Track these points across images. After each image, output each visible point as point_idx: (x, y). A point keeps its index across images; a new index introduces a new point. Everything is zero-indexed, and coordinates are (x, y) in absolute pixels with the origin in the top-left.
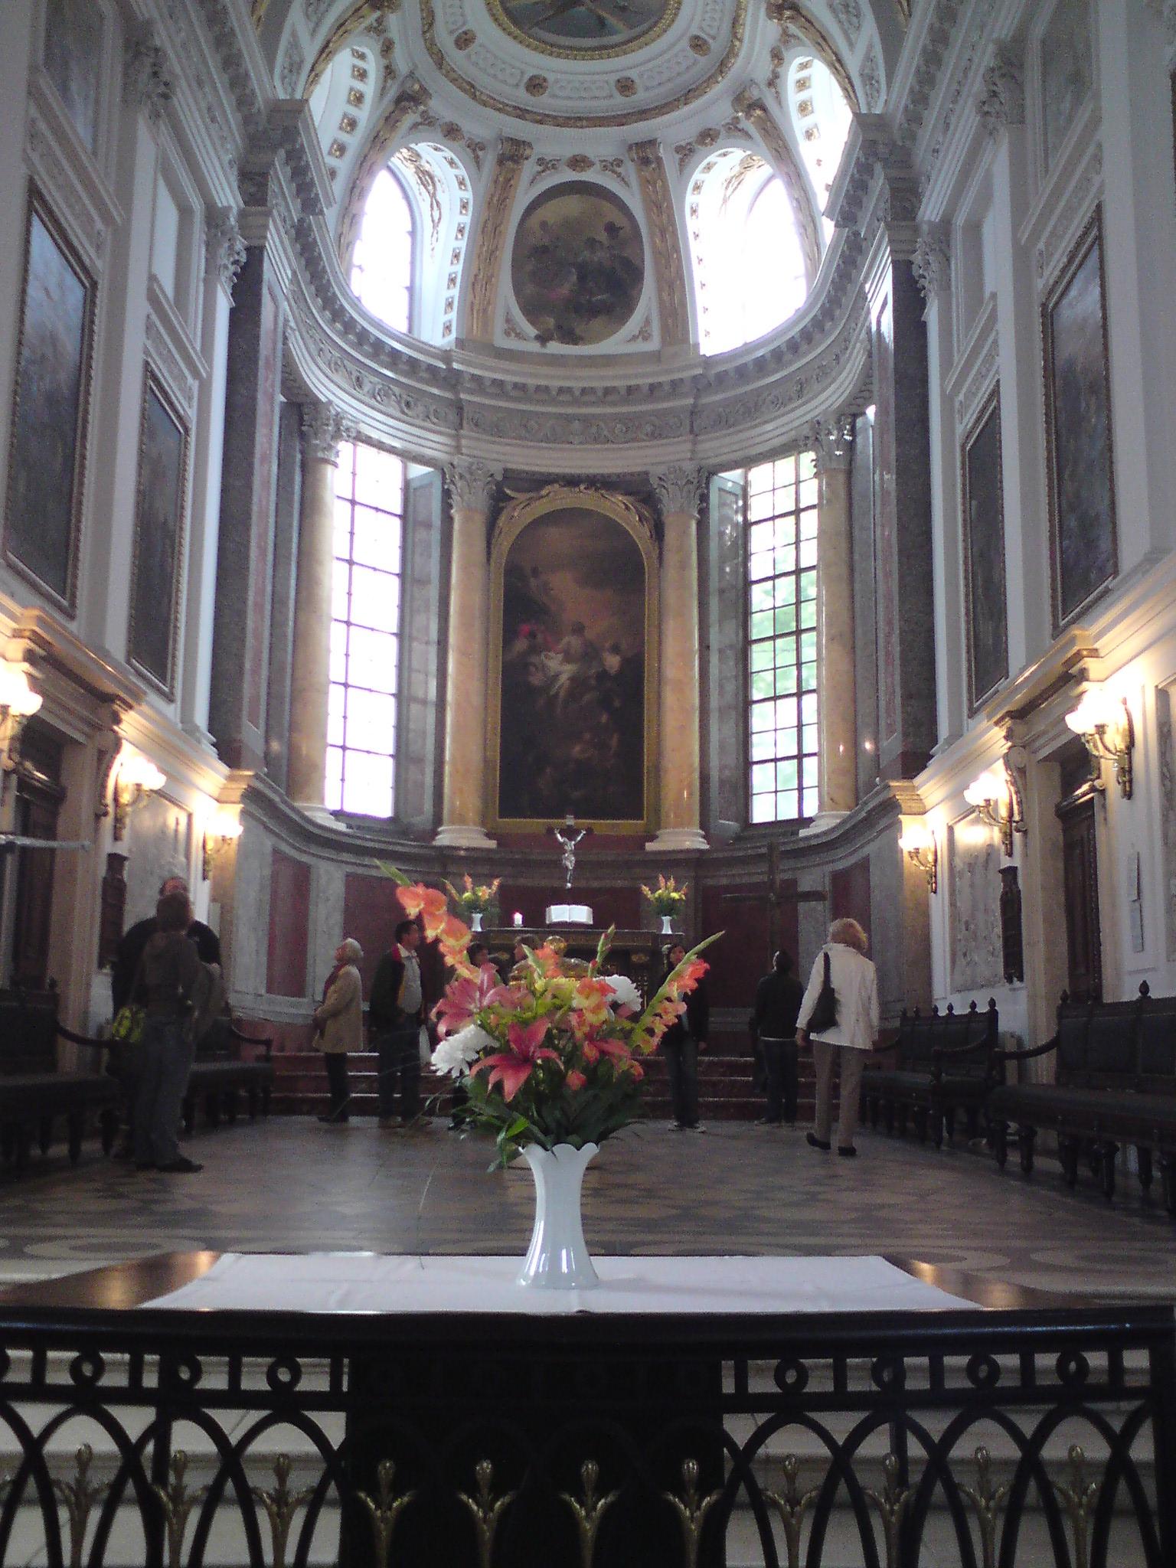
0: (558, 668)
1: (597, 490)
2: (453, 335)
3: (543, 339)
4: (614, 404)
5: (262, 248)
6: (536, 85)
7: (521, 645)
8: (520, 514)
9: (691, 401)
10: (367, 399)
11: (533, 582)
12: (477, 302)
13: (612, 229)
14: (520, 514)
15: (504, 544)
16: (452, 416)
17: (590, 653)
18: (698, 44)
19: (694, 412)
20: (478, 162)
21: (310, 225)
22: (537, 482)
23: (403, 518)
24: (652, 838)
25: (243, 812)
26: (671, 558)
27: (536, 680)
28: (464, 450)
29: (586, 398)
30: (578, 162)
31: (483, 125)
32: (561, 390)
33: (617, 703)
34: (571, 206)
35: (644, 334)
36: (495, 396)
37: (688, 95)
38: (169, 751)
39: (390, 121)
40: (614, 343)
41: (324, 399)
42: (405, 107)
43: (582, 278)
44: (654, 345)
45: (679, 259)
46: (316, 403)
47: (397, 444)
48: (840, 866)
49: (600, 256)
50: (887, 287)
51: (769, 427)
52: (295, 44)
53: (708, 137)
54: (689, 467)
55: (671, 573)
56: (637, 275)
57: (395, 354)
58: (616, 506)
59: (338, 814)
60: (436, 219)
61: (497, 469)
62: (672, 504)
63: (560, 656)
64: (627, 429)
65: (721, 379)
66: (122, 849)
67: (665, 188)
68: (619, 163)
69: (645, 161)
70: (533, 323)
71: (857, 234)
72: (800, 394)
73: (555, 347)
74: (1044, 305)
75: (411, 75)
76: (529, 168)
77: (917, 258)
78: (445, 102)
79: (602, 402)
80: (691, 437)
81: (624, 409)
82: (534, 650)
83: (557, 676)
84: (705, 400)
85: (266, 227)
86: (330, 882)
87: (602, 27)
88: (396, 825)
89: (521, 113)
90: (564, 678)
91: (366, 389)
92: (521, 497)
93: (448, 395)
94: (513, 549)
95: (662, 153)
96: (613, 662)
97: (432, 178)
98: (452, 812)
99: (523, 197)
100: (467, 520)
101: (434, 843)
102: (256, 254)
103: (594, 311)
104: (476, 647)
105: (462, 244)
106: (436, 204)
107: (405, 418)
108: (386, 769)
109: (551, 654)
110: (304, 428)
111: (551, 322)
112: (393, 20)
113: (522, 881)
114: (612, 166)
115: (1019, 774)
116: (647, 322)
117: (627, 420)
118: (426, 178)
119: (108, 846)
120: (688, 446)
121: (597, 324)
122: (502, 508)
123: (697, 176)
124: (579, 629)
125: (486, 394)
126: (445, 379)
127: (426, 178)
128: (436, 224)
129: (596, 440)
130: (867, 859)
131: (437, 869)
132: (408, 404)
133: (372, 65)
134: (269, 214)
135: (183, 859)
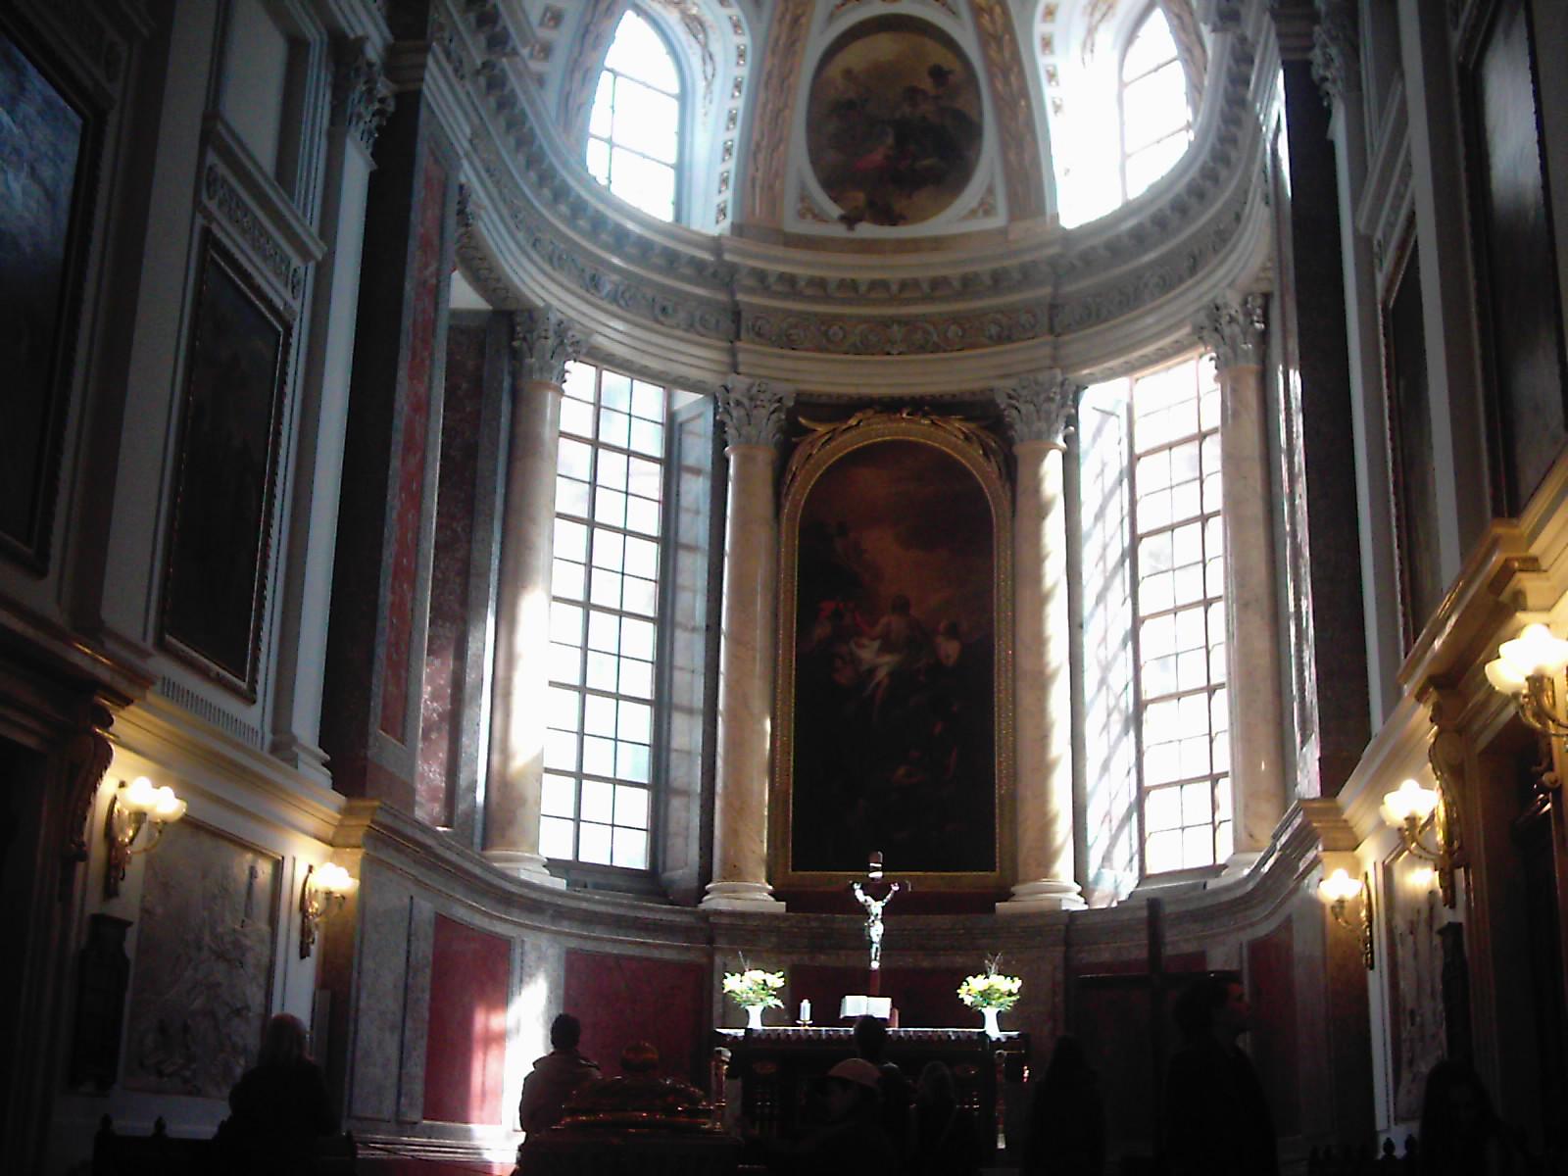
1: (925, 415)
3: (850, 220)
5: (417, 95)
7: (822, 630)
9: (1046, 291)
10: (605, 304)
12: (759, 175)
13: (939, 74)
15: (800, 492)
16: (727, 324)
19: (1054, 308)
21: (503, 70)
24: (1007, 896)
28: (741, 369)
29: (906, 295)
32: (874, 285)
34: (884, 47)
36: (785, 296)
40: (951, 220)
41: (541, 304)
44: (998, 220)
45: (1029, 106)
47: (655, 364)
48: (1262, 930)
50: (1278, 107)
51: (1150, 320)
56: (972, 131)
59: (554, 866)
60: (710, 77)
61: (786, 389)
63: (876, 644)
64: (964, 330)
67: (1006, 12)
70: (835, 200)
71: (1243, 40)
72: (1193, 270)
73: (866, 230)
74: (1462, 68)
77: (1317, 55)
79: (926, 299)
80: (1050, 338)
83: (872, 671)
84: (1070, 288)
85: (423, 66)
88: (650, 882)
91: (604, 292)
92: (821, 429)
93: (722, 297)
96: (950, 649)
97: (701, 24)
98: (724, 862)
100: (744, 461)
101: (702, 906)
104: (760, 636)
106: (708, 57)
107: (657, 326)
108: (636, 806)
109: (865, 641)
110: (516, 344)
111: (860, 198)
113: (822, 959)
115: (1453, 773)
116: (990, 190)
122: (796, 445)
124: (902, 606)
125: (775, 295)
126: (715, 275)
129: (922, 349)
130: (1289, 919)
132: (664, 310)
134: (427, 49)
135: (264, 927)
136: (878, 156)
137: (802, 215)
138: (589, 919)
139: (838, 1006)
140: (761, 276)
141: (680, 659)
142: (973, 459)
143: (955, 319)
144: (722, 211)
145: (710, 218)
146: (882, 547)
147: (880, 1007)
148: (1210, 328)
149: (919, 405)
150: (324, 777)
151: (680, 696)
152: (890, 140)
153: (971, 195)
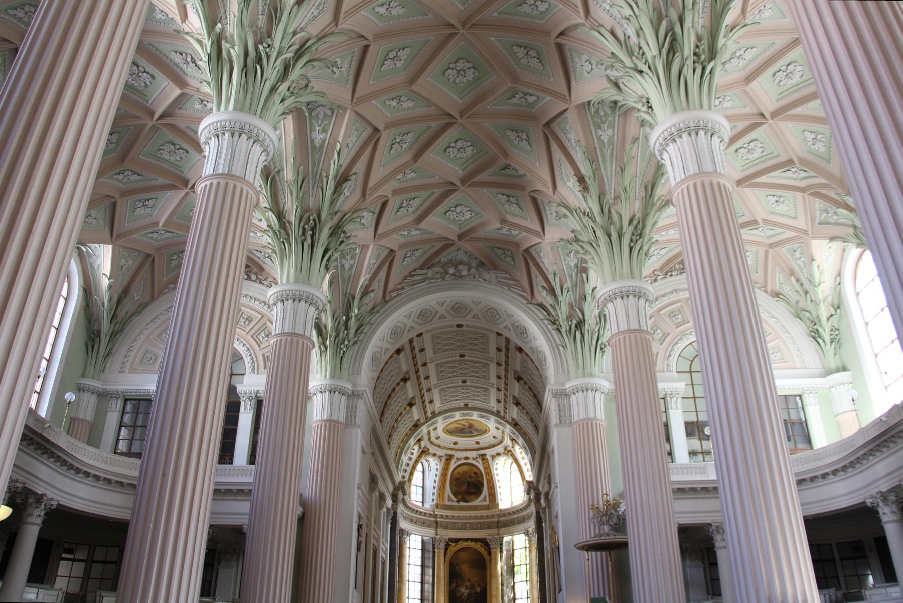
0: (464, 591)
3: (458, 502)
6: (455, 443)
7: (454, 585)
9: (496, 520)
13: (475, 473)
14: (454, 548)
18: (494, 437)
19: (498, 522)
22: (456, 541)
23: (422, 550)
26: (493, 562)
27: (458, 595)
30: (466, 458)
35: (484, 500)
37: (493, 446)
39: (420, 457)
42: (424, 452)
43: (468, 485)
44: (487, 503)
53: (498, 454)
56: (482, 485)
57: (421, 512)
58: (478, 546)
65: (504, 515)
73: (461, 504)
76: (453, 460)
82: (457, 586)
89: (452, 449)
96: (478, 589)
99: (452, 466)
102: (395, 513)
103: (471, 494)
105: (437, 479)
106: (429, 466)
111: (460, 497)
114: (474, 459)
118: (428, 461)
121: (472, 497)
124: (469, 581)
127: (428, 461)
128: (430, 471)
133: (416, 447)
141: (426, 590)
143: (479, 523)
146: (465, 569)
148: (527, 533)
149: (472, 540)
151: (426, 598)
153: (482, 497)
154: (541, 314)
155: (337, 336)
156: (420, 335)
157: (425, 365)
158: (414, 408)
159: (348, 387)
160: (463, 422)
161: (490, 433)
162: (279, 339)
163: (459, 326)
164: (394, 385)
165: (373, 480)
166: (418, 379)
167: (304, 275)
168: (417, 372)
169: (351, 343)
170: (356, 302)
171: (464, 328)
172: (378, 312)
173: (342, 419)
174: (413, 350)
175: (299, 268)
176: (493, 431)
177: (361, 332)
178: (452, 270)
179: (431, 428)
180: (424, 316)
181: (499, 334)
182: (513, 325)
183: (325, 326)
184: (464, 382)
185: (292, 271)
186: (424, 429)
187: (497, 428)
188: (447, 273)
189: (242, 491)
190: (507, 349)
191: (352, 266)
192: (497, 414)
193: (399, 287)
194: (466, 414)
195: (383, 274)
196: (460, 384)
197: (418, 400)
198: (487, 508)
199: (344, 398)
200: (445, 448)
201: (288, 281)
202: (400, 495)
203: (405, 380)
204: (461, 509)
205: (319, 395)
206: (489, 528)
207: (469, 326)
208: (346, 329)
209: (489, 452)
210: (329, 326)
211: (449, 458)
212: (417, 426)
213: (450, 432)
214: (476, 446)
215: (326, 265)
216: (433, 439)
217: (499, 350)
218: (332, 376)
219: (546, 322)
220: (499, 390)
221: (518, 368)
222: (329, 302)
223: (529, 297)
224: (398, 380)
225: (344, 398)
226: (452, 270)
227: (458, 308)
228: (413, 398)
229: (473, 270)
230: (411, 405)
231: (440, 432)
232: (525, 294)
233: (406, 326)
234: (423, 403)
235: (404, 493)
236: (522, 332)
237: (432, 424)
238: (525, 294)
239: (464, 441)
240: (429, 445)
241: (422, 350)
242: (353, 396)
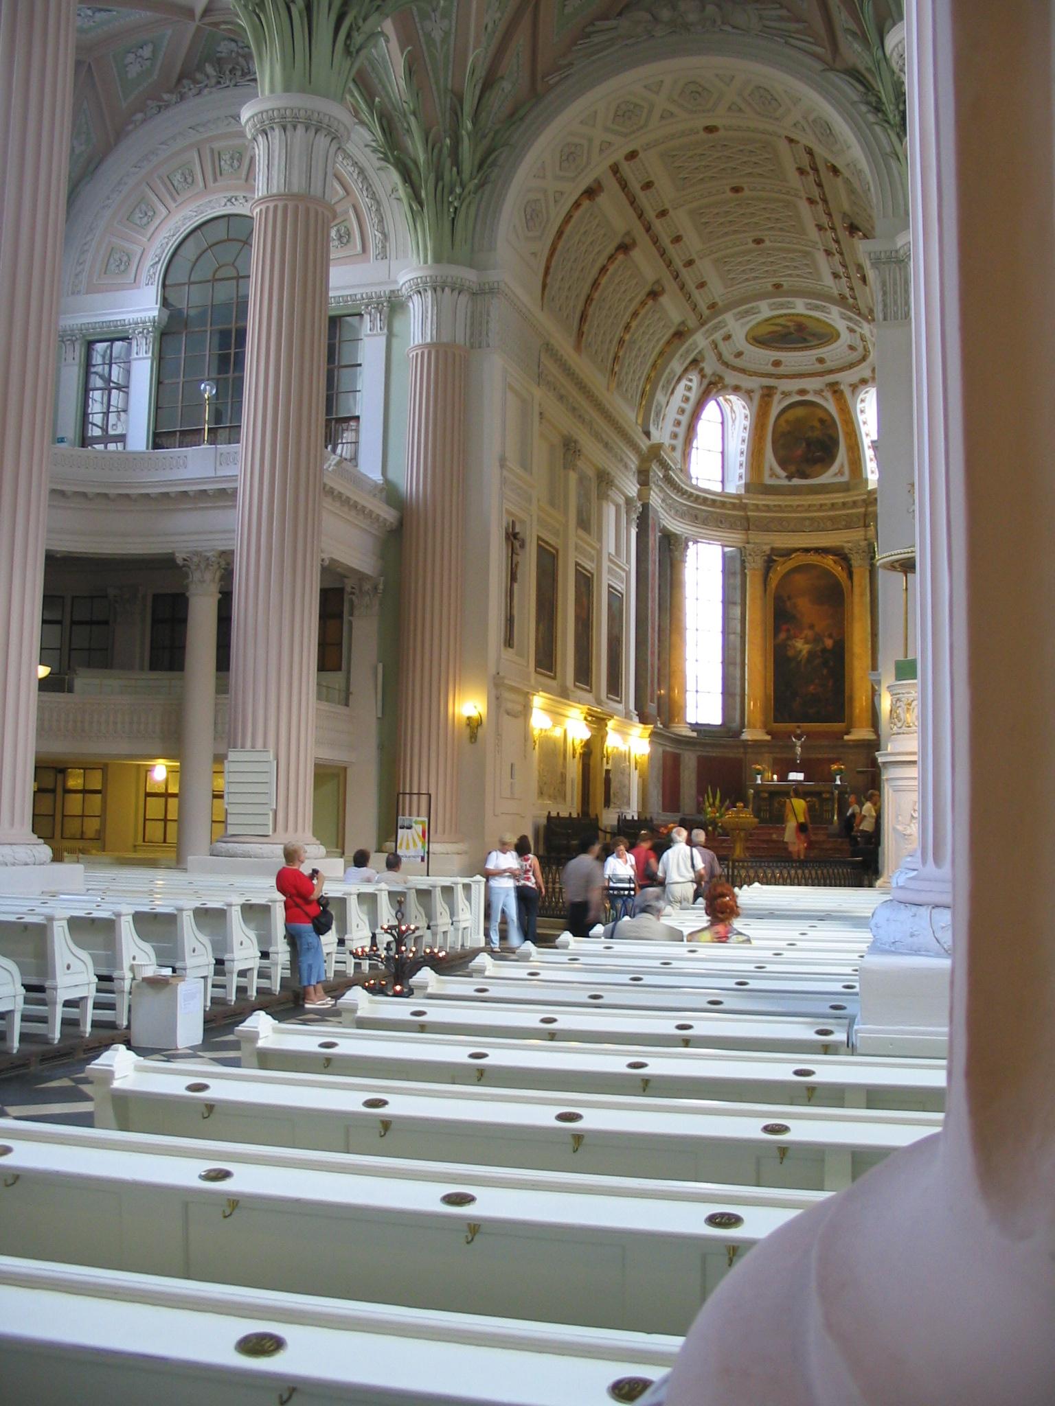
0: (801, 646)
2: (743, 482)
3: (789, 477)
4: (826, 511)
6: (777, 363)
7: (782, 636)
8: (781, 569)
9: (862, 510)
11: (788, 604)
13: (822, 421)
14: (781, 569)
17: (817, 639)
18: (851, 348)
19: (865, 515)
20: (751, 399)
24: (847, 733)
25: (651, 742)
26: (857, 590)
27: (791, 653)
30: (802, 392)
31: (754, 383)
33: (831, 664)
35: (841, 473)
37: (851, 366)
38: (622, 733)
40: (826, 478)
42: (712, 388)
43: (808, 445)
46: (675, 535)
49: (817, 434)
52: (659, 404)
53: (864, 382)
54: (863, 543)
55: (856, 599)
56: (835, 443)
58: (829, 562)
61: (767, 548)
62: (856, 562)
66: (609, 767)
68: (822, 391)
69: (835, 392)
75: (713, 374)
76: (777, 397)
78: (731, 378)
81: (831, 513)
82: (788, 638)
86: (690, 761)
87: (805, 340)
90: (804, 652)
93: (742, 513)
94: (777, 587)
95: (842, 387)
96: (829, 643)
99: (775, 410)
102: (646, 506)
106: (732, 410)
111: (793, 468)
112: (702, 365)
114: (818, 392)
116: (842, 466)
117: (831, 519)
119: (605, 767)
120: (862, 533)
121: (818, 467)
123: (862, 396)
124: (812, 627)
128: (734, 421)
131: (742, 750)
133: (694, 377)
136: (799, 452)
137: (771, 476)
138: (704, 745)
139: (787, 776)
140: (757, 505)
142: (838, 571)
144: (741, 477)
145: (735, 486)
146: (804, 606)
147: (800, 776)
150: (636, 719)
152: (804, 445)
153: (835, 467)
154: (852, 92)
155: (439, 178)
156: (632, 155)
157: (663, 214)
158: (664, 300)
159: (469, 276)
160: (781, 321)
161: (839, 343)
162: (263, 207)
163: (710, 129)
164: (602, 260)
165: (570, 449)
166: (655, 241)
167: (300, 78)
168: (648, 229)
169: (471, 186)
170: (468, 108)
171: (722, 133)
172: (522, 119)
173: (460, 339)
174: (624, 185)
175: (289, 64)
176: (845, 338)
177: (494, 164)
178: (665, 14)
179: (718, 336)
180: (626, 113)
181: (791, 141)
182: (805, 118)
183: (415, 163)
184: (758, 241)
185: (278, 67)
186: (700, 340)
187: (852, 330)
188: (656, 19)
189: (166, 495)
190: (816, 170)
191: (447, 34)
192: (842, 301)
193: (563, 62)
194: (782, 306)
195: (521, 41)
196: (752, 246)
197: (670, 285)
198: (845, 488)
199: (464, 299)
200: (755, 374)
201: (272, 91)
202: (657, 472)
203: (624, 248)
204: (795, 491)
205: (416, 298)
206: (848, 527)
207: (726, 129)
208: (456, 162)
209: (846, 378)
210: (422, 158)
211: (768, 393)
212: (680, 335)
213: (759, 341)
214: (819, 367)
215: (347, 47)
216: (728, 357)
217: (801, 171)
218: (438, 259)
219: (864, 108)
220: (828, 253)
221: (846, 207)
222: (414, 113)
223: (829, 58)
224: (610, 249)
225: (464, 299)
226: (665, 14)
227: (695, 92)
228: (657, 282)
229: (710, 9)
230: (654, 294)
231: (740, 340)
232: (819, 50)
233: (590, 140)
234: (682, 287)
235: (665, 467)
236: (826, 131)
237: (716, 328)
238: (819, 50)
239: (794, 359)
240: (721, 369)
241: (648, 186)
242: (481, 293)
